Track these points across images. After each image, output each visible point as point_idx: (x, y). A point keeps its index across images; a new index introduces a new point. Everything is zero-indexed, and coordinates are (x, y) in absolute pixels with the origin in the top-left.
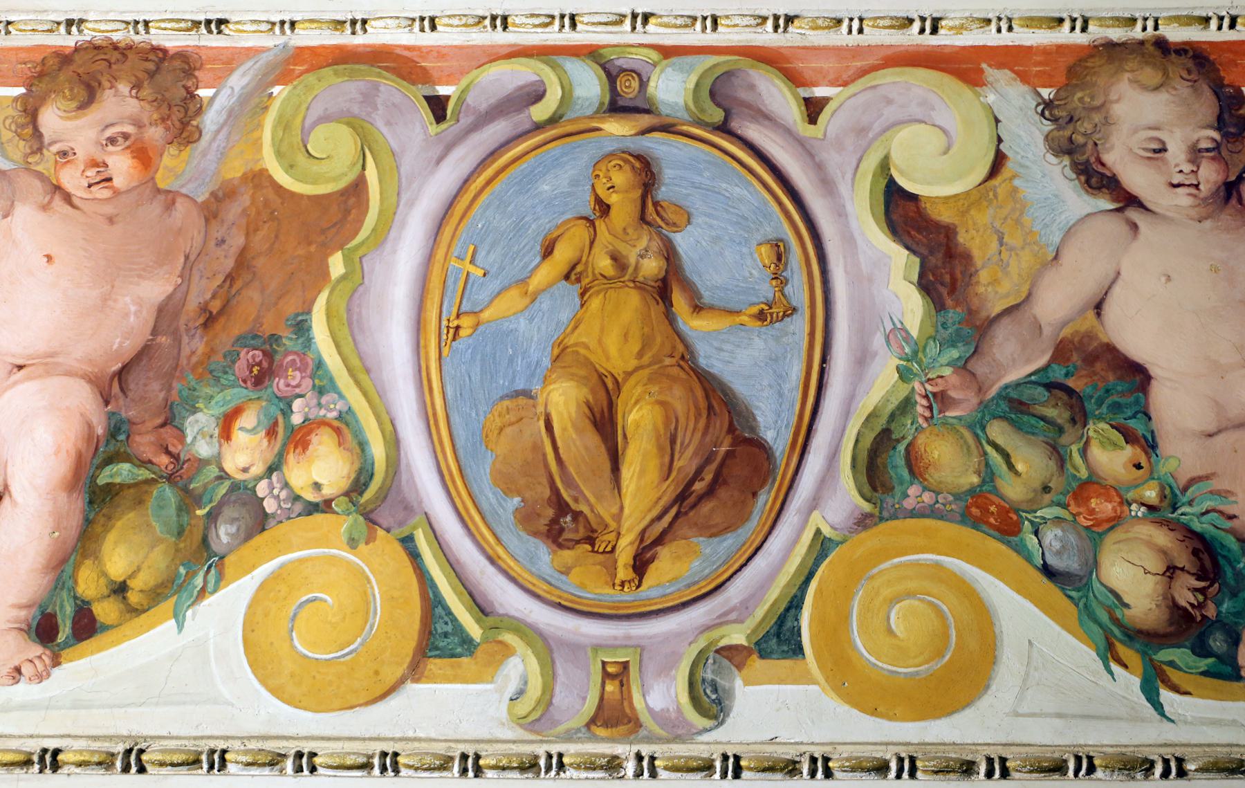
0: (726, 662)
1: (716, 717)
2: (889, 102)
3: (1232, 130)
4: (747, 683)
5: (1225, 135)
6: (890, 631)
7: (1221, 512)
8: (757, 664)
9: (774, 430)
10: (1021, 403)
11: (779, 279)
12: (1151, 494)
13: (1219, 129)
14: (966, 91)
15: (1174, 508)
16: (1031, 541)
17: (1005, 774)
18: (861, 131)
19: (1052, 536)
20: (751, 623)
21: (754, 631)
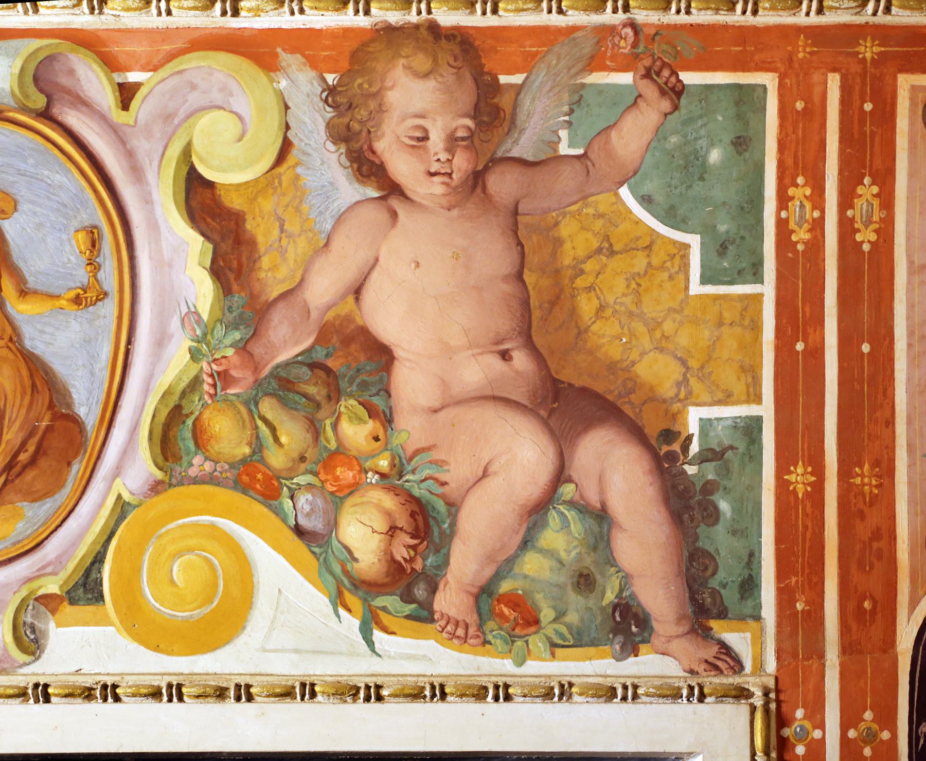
0: (43, 608)
1: (33, 654)
2: (193, 87)
3: (485, 119)
4: (59, 625)
6: (173, 582)
7: (436, 480)
8: (67, 609)
9: (86, 407)
10: (289, 381)
11: (93, 265)
12: (384, 463)
13: (474, 118)
14: (262, 77)
15: (401, 476)
16: (287, 504)
17: (250, 698)
18: (168, 117)
19: (304, 499)
20: (63, 575)
21: (65, 582)
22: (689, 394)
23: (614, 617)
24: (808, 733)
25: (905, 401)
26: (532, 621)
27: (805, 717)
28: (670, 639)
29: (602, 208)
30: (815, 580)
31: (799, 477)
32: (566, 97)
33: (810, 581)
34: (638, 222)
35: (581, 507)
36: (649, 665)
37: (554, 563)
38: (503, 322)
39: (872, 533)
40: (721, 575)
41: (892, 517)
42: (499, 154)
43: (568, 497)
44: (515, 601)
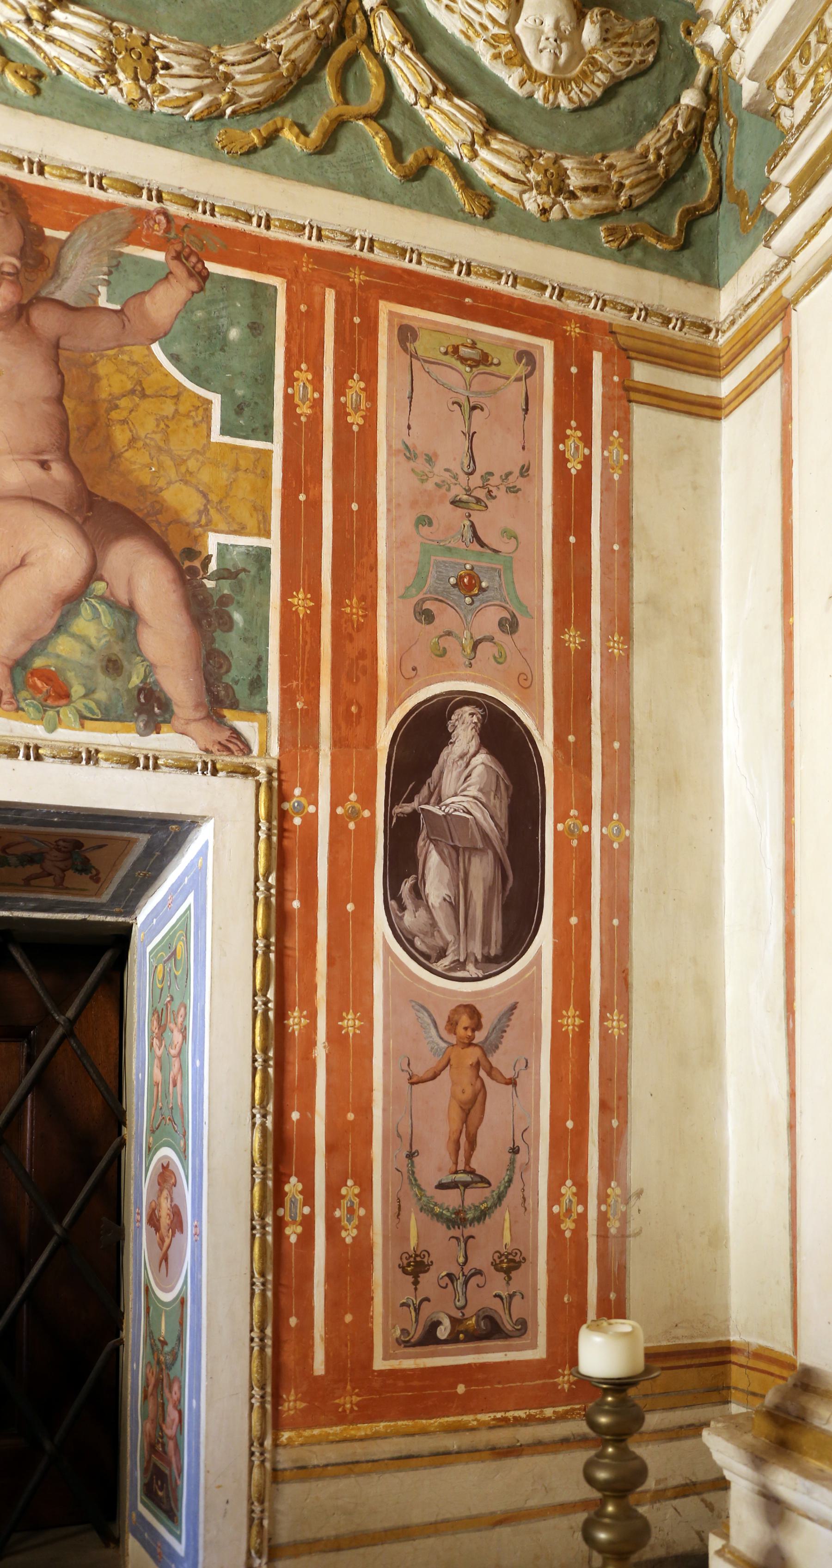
3: (31, 262)
5: (25, 264)
13: (20, 258)
22: (209, 522)
23: (139, 699)
24: (304, 808)
25: (385, 552)
26: (63, 695)
27: (301, 795)
28: (188, 722)
29: (136, 358)
30: (312, 685)
31: (300, 600)
32: (105, 260)
33: (308, 685)
34: (167, 375)
35: (112, 603)
36: (167, 741)
37: (85, 648)
38: (43, 436)
39: (359, 653)
40: (233, 673)
41: (375, 642)
42: (43, 294)
43: (100, 593)
44: (47, 676)
